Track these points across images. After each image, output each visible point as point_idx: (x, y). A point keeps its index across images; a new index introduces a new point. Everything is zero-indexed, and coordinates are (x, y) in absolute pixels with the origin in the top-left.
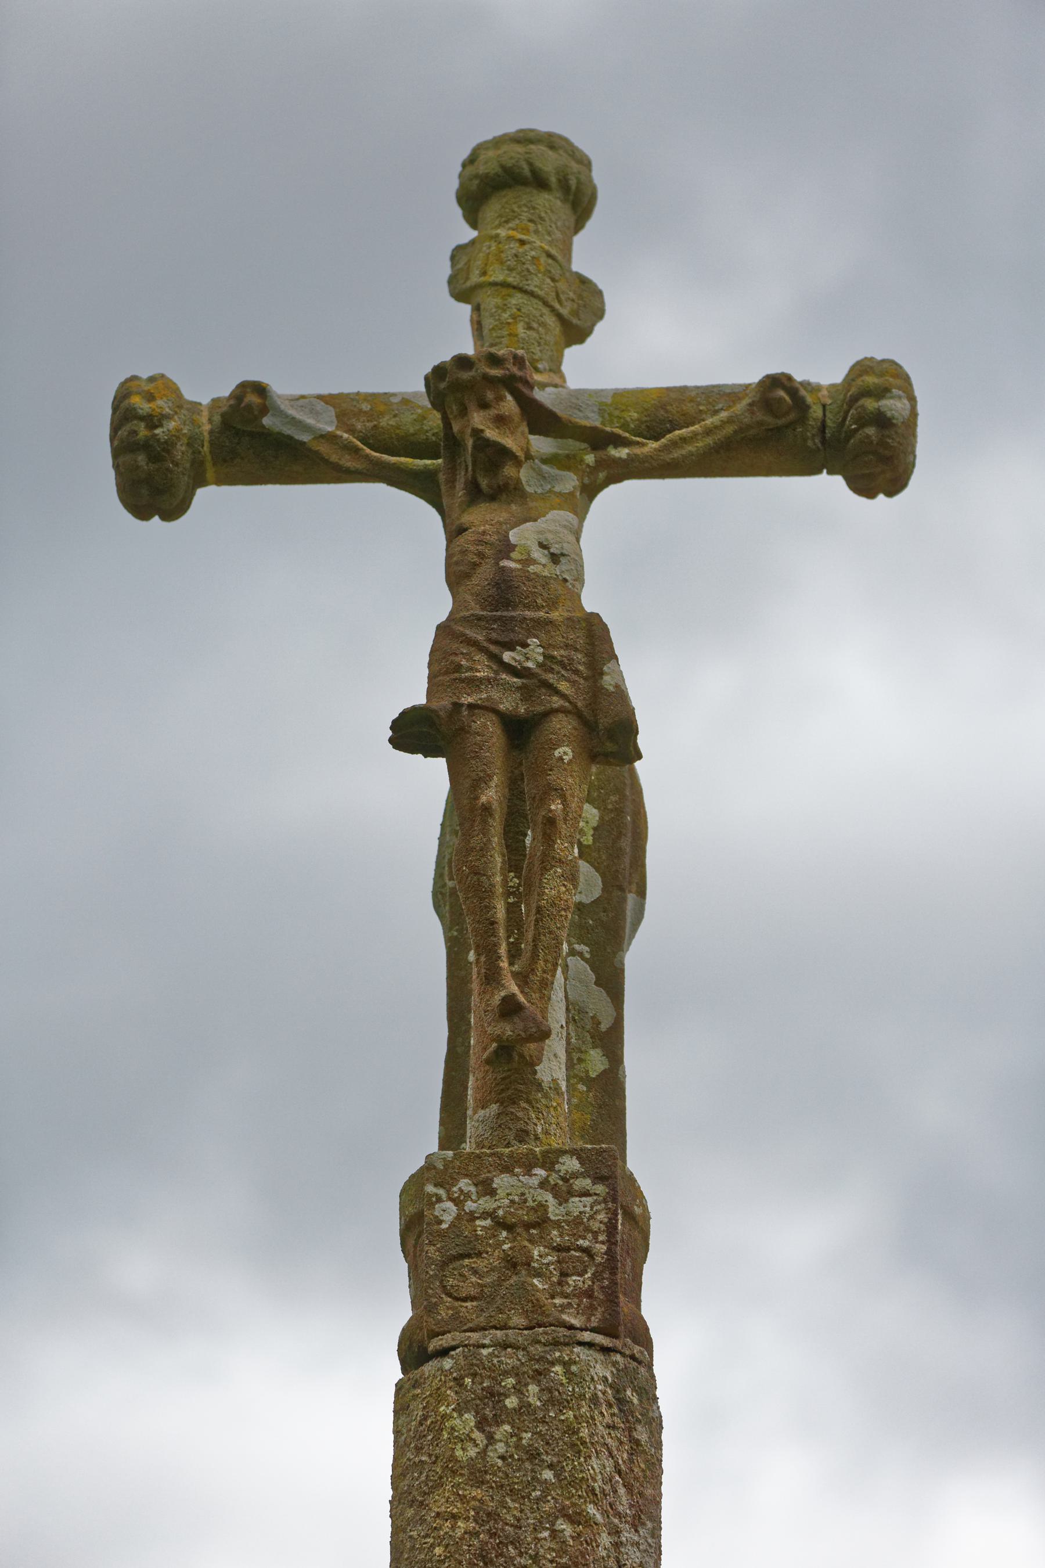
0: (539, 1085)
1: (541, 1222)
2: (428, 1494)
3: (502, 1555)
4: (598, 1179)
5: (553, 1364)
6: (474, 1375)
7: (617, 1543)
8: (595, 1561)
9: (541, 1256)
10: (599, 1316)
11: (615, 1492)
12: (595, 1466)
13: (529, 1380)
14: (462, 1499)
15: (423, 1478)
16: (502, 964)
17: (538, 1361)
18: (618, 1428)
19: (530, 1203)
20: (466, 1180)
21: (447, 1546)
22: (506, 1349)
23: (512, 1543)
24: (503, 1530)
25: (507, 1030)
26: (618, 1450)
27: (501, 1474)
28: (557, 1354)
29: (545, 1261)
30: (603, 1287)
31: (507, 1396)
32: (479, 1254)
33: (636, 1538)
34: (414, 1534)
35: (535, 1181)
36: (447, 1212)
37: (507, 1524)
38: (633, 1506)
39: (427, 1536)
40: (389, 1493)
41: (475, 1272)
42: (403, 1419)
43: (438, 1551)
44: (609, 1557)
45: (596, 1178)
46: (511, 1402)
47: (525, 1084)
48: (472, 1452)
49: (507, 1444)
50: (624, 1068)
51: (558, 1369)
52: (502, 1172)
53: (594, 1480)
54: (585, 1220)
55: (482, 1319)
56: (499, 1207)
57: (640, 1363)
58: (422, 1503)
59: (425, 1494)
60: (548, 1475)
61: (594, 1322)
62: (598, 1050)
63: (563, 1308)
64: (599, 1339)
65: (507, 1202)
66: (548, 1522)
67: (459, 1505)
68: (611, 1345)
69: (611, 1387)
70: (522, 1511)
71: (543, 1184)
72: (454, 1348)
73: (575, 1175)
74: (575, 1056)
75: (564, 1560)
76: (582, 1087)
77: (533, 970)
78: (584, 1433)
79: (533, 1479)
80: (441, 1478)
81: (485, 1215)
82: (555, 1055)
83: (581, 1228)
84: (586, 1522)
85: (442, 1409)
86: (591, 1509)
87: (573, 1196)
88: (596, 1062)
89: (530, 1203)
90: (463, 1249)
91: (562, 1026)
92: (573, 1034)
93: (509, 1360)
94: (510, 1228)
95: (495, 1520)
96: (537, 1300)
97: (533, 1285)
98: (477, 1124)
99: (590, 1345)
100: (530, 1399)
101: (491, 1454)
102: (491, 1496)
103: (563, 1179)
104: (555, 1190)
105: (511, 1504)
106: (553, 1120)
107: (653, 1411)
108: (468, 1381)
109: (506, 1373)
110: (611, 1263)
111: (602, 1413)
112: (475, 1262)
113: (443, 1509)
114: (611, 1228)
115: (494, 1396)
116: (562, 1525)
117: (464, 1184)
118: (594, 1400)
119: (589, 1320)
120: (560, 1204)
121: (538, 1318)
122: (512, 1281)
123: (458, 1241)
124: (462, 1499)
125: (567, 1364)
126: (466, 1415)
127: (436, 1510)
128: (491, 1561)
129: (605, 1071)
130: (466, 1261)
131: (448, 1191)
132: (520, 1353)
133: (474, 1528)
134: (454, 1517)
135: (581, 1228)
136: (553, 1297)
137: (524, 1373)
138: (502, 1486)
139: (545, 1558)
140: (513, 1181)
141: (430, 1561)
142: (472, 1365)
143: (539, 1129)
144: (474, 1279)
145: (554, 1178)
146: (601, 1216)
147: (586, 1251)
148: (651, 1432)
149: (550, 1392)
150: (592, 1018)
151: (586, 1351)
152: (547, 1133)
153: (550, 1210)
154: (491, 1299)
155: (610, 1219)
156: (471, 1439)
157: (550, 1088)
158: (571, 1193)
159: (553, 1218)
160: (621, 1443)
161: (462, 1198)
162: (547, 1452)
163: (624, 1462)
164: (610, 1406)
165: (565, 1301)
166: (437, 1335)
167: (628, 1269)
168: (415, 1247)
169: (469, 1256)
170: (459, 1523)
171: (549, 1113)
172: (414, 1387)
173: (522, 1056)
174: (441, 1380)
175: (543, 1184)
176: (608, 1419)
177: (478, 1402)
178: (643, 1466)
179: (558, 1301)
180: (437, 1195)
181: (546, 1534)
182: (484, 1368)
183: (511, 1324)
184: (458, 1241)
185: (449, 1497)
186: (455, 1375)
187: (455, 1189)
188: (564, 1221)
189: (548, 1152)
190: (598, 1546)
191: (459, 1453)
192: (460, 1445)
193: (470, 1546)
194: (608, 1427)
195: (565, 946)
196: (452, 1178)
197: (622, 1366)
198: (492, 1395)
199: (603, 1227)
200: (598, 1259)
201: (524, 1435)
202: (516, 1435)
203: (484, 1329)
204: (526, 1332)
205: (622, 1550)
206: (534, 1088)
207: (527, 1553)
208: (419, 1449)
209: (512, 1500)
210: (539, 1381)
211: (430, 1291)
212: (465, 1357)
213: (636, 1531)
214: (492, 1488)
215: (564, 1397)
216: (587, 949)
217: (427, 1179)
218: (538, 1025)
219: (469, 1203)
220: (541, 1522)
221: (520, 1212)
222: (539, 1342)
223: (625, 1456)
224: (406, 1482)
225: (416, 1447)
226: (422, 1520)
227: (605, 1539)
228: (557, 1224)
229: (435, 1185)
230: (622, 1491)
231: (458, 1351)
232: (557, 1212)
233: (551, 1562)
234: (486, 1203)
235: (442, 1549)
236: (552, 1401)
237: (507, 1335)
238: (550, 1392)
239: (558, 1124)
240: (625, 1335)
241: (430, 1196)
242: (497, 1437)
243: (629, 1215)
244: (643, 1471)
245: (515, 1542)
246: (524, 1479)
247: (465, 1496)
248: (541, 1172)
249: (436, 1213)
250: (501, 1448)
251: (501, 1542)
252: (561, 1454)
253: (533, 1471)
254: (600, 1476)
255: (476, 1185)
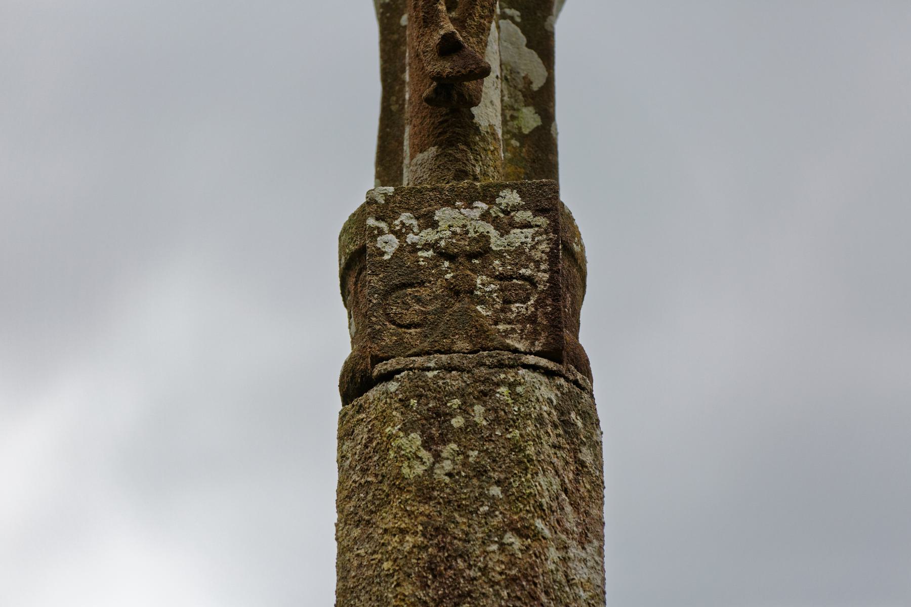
0: (476, 129)
1: (482, 251)
2: (375, 513)
3: (450, 567)
4: (539, 211)
5: (498, 385)
6: (419, 397)
7: (564, 558)
8: (544, 573)
9: (483, 285)
10: (543, 340)
11: (562, 509)
12: (542, 483)
13: (475, 401)
14: (410, 514)
15: (370, 497)
16: (440, 7)
17: (483, 382)
18: (563, 449)
19: (472, 234)
20: (408, 214)
21: (395, 560)
22: (450, 372)
23: (461, 556)
24: (451, 543)
25: (446, 67)
26: (564, 470)
27: (448, 490)
28: (502, 376)
29: (488, 289)
30: (546, 313)
31: (453, 416)
32: (422, 284)
33: (584, 555)
34: (362, 552)
35: (476, 213)
36: (389, 244)
37: (455, 538)
38: (580, 524)
39: (375, 552)
40: (334, 517)
41: (419, 300)
42: (348, 443)
43: (386, 565)
44: (557, 570)
45: (537, 210)
46: (457, 422)
47: (462, 127)
48: (419, 469)
49: (453, 461)
50: (556, 125)
51: (503, 390)
52: (443, 206)
53: (542, 496)
54: (527, 250)
55: (426, 344)
56: (441, 238)
57: (583, 389)
58: (368, 522)
59: (372, 512)
60: (496, 491)
61: (538, 347)
62: (531, 109)
63: (507, 334)
64: (543, 362)
65: (448, 233)
66: (497, 536)
67: (407, 520)
68: (555, 368)
69: (555, 408)
70: (469, 526)
71: (485, 216)
72: (399, 371)
73: (516, 208)
74: (508, 113)
75: (513, 572)
76: (515, 143)
77: (470, 14)
78: (531, 450)
79: (480, 494)
80: (388, 495)
81: (427, 246)
82: (491, 102)
83: (523, 258)
84: (535, 536)
85: (387, 430)
86: (539, 524)
87: (514, 228)
88: (529, 119)
89: (472, 234)
90: (404, 277)
91: (497, 77)
92: (506, 92)
93: (455, 381)
94: (452, 258)
95: (443, 534)
96: (481, 325)
97: (476, 311)
98: (415, 168)
99: (534, 368)
100: (475, 419)
101: (438, 471)
102: (439, 512)
103: (503, 211)
104: (496, 222)
105: (459, 519)
106: (491, 163)
107: (597, 435)
108: (413, 402)
109: (452, 395)
110: (555, 291)
111: (547, 432)
112: (418, 291)
113: (391, 525)
114: (553, 257)
115: (441, 416)
116: (509, 538)
117: (405, 217)
118: (540, 420)
119: (533, 344)
120: (502, 236)
121: (482, 340)
122: (455, 308)
123: (400, 271)
124: (410, 514)
125: (512, 386)
126: (412, 435)
127: (384, 526)
128: (441, 575)
129: (537, 128)
130: (409, 290)
131: (390, 225)
132: (466, 376)
133: (423, 542)
134: (403, 532)
135: (523, 258)
136: (496, 323)
137: (470, 393)
138: (449, 502)
139: (494, 570)
140: (455, 213)
141: (379, 576)
142: (417, 387)
143: (478, 170)
144: (417, 307)
145: (494, 211)
146: (544, 246)
147: (529, 279)
148: (596, 455)
149: (496, 411)
150: (524, 78)
151: (531, 374)
152: (485, 174)
153: (492, 240)
154: (434, 325)
155: (551, 249)
156: (418, 457)
157: (487, 132)
158: (513, 225)
159: (494, 248)
160: (567, 463)
161: (404, 230)
162: (493, 469)
163: (570, 481)
164: (555, 426)
165: (509, 327)
166: (381, 360)
167: (568, 304)
168: (356, 284)
169: (411, 285)
170: (407, 538)
171: (487, 155)
172: (358, 412)
173: (461, 95)
174: (386, 403)
175: (485, 216)
176: (553, 439)
177: (424, 422)
178: (588, 486)
179: (501, 327)
180: (378, 228)
181: (494, 547)
182: (430, 390)
183: (455, 348)
184: (400, 271)
185: (397, 514)
186: (400, 396)
187: (397, 222)
188: (506, 251)
189: (488, 186)
190: (546, 560)
191: (405, 471)
192: (406, 463)
193: (419, 559)
194: (554, 446)
195: (498, 11)
196: (394, 212)
197: (566, 390)
198: (438, 415)
199: (545, 257)
200: (541, 287)
201: (471, 453)
202: (463, 453)
203: (428, 353)
204: (470, 356)
205: (570, 564)
206: (472, 131)
207: (475, 566)
208: (364, 471)
209: (461, 516)
210: (485, 402)
211: (374, 319)
212: (411, 380)
213: (584, 548)
214: (439, 503)
215: (510, 416)
216: (518, 13)
217: (369, 213)
218: (478, 62)
219: (411, 235)
220: (489, 536)
221: (462, 243)
222: (484, 365)
223: (571, 476)
224: (353, 503)
225: (362, 470)
226: (370, 538)
227: (553, 554)
228: (499, 255)
229: (377, 219)
230: (568, 509)
231: (403, 374)
232: (499, 243)
233: (501, 573)
234: (429, 235)
235: (390, 563)
236: (497, 421)
237: (451, 358)
238: (496, 411)
239: (495, 167)
240: (565, 358)
241: (372, 229)
242: (445, 454)
243: (569, 251)
244: (589, 491)
245: (464, 555)
246: (472, 495)
247: (413, 512)
248: (483, 206)
249: (378, 245)
250: (448, 465)
251: (449, 556)
252: (508, 471)
253: (480, 487)
254: (547, 493)
255: (417, 218)
